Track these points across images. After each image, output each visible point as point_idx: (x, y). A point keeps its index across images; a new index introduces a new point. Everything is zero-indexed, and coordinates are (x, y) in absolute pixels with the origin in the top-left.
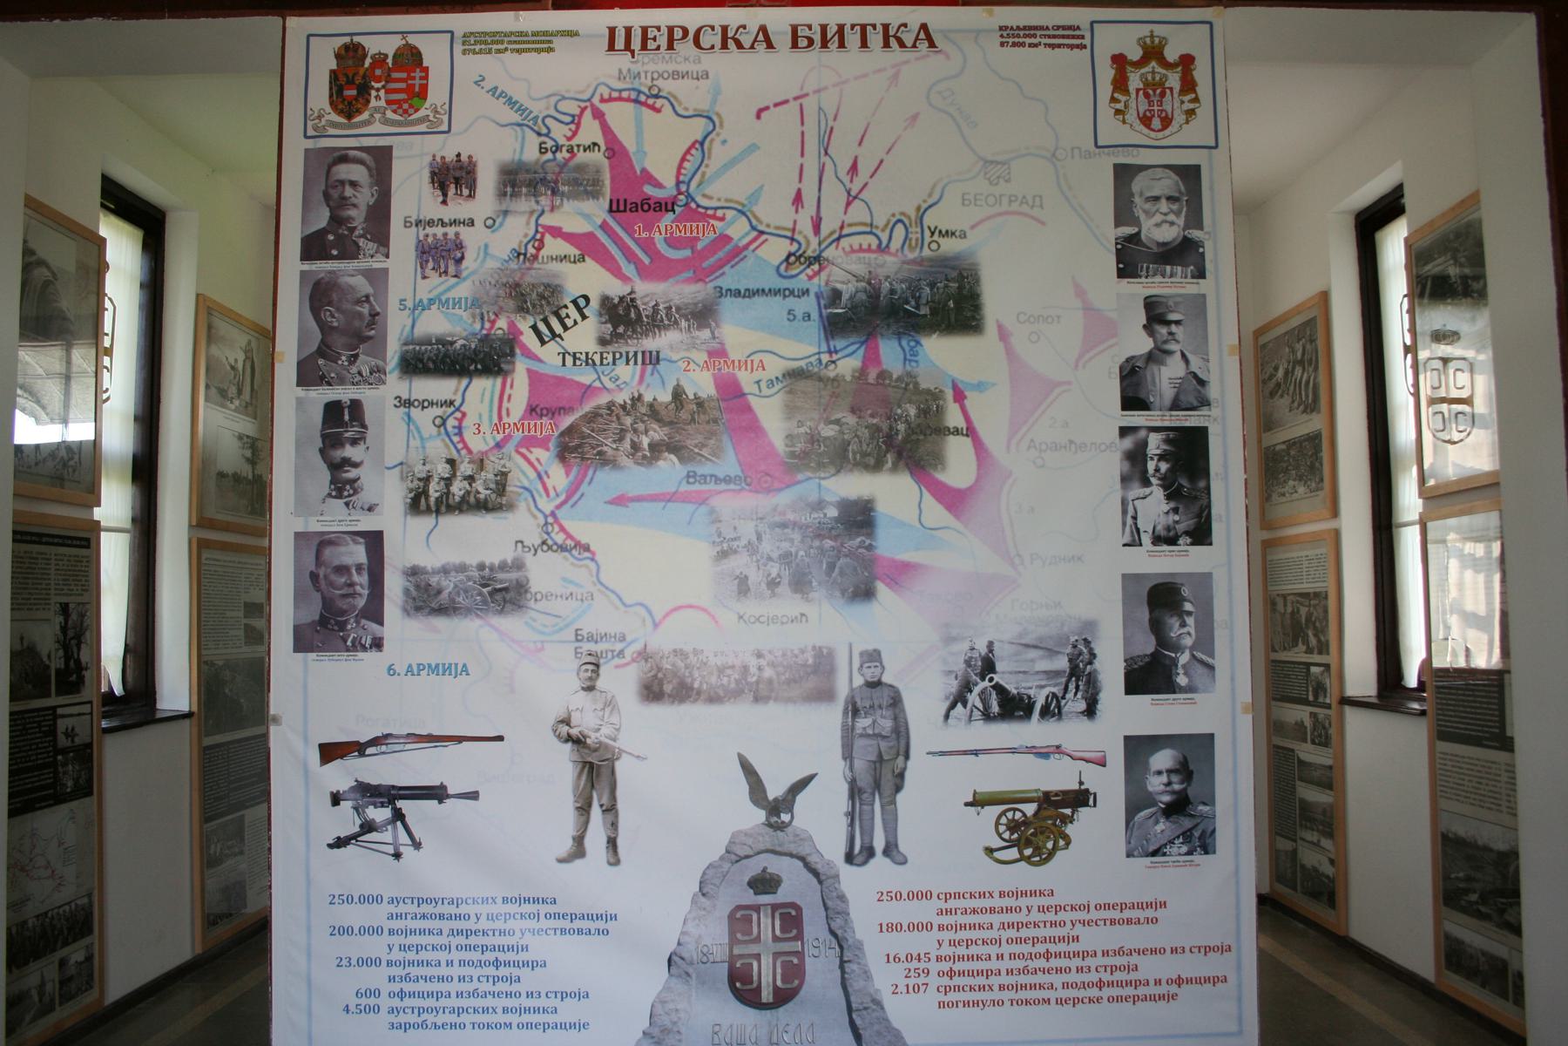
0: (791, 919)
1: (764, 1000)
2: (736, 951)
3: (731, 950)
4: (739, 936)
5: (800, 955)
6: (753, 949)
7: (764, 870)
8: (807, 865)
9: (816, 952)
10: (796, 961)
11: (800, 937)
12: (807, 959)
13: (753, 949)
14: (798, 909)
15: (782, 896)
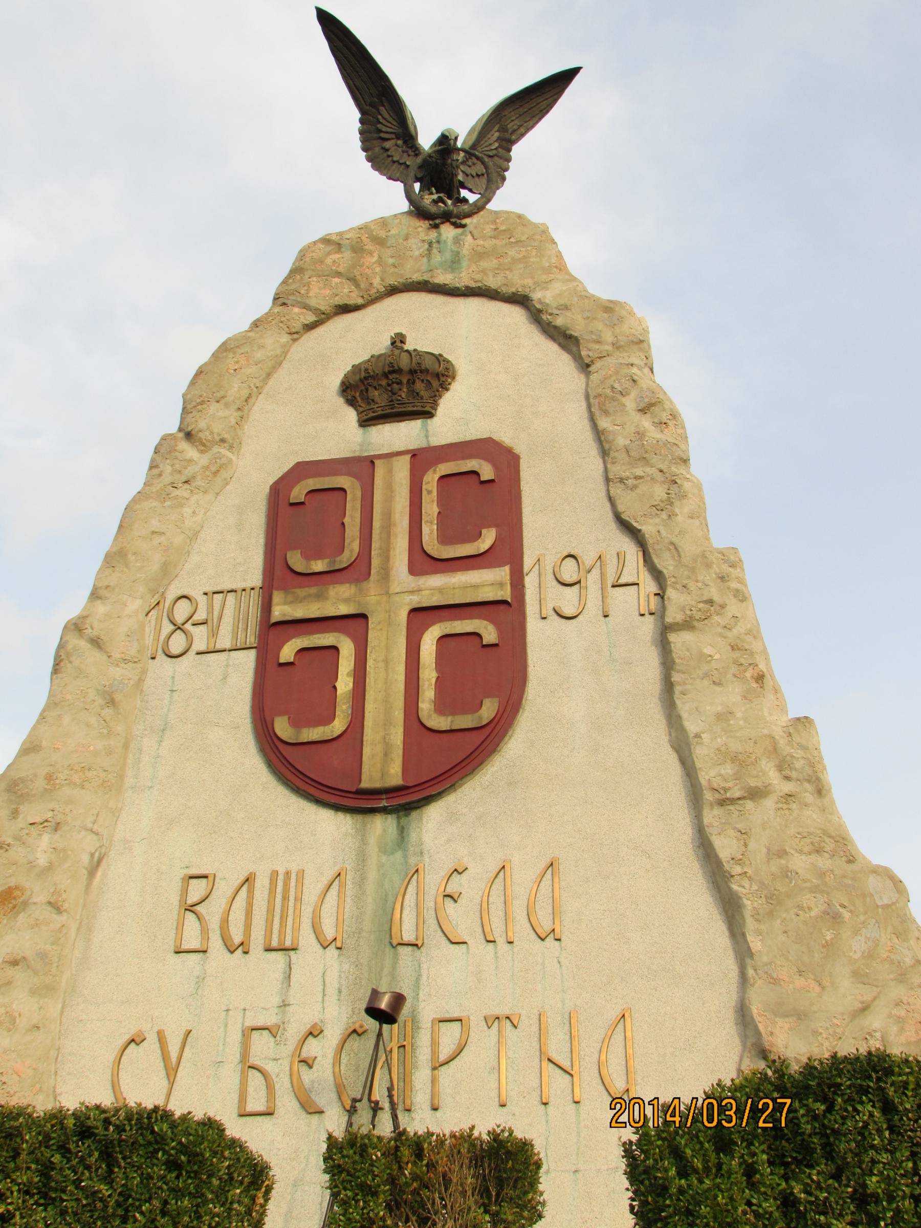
0: (480, 494)
1: (370, 779)
2: (280, 611)
3: (267, 607)
4: (297, 561)
5: (508, 610)
6: (339, 600)
7: (398, 340)
8: (536, 316)
9: (568, 600)
10: (490, 634)
11: (509, 551)
12: (533, 625)
13: (339, 600)
14: (507, 460)
15: (456, 417)
